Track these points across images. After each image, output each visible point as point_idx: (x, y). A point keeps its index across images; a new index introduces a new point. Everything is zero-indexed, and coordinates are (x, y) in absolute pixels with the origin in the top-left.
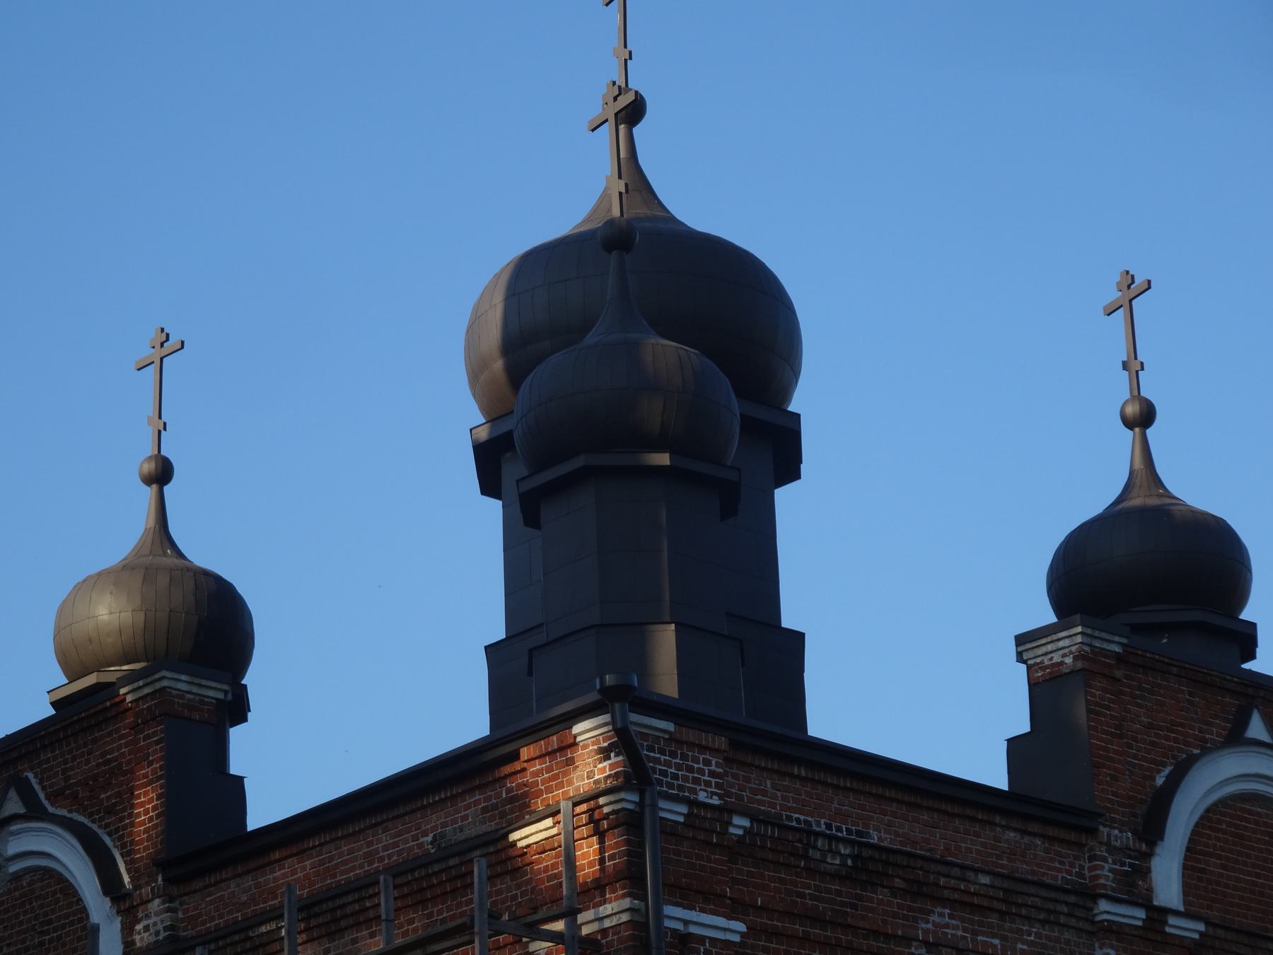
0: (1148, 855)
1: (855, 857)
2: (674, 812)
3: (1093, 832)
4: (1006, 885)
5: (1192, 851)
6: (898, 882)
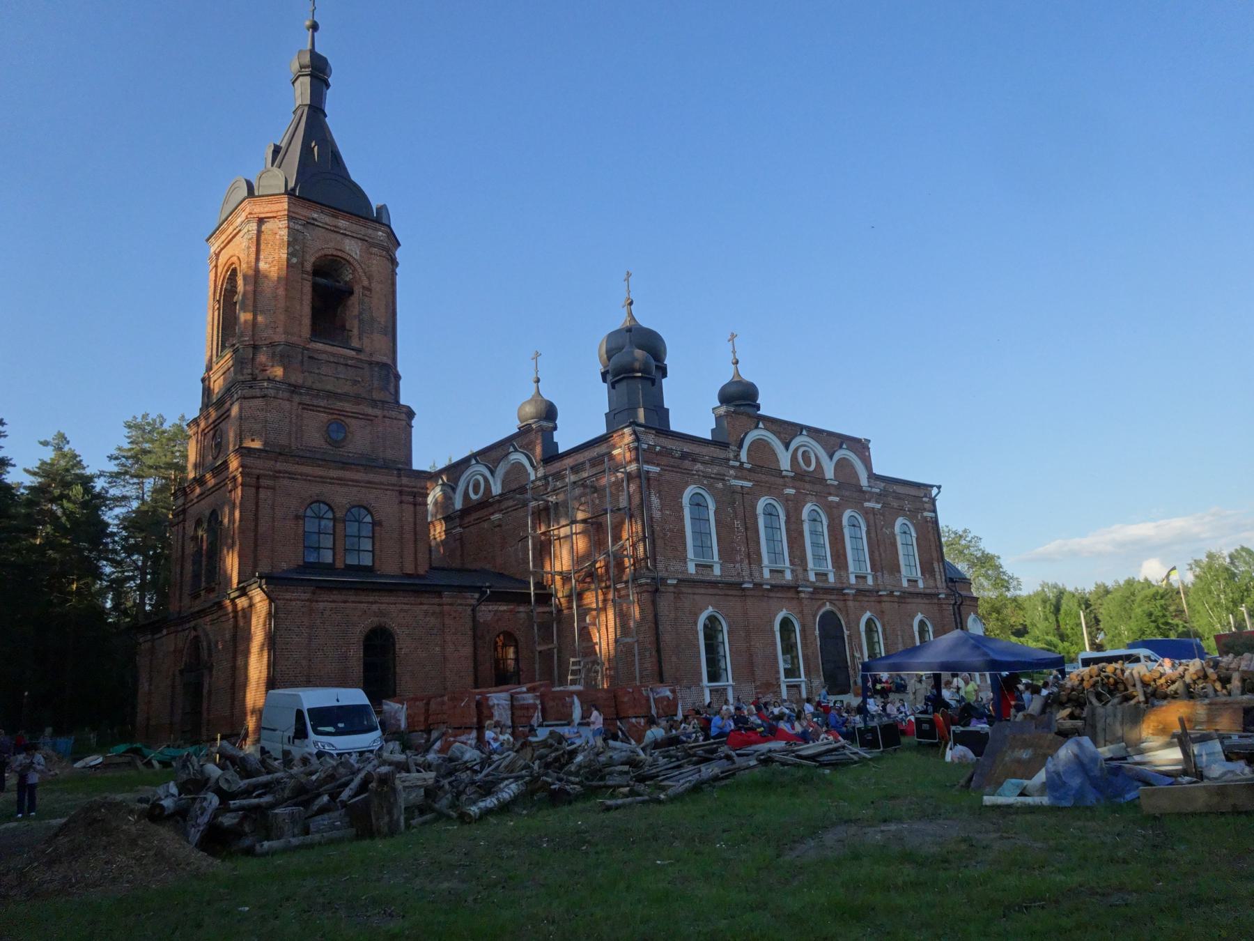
2: (645, 446)
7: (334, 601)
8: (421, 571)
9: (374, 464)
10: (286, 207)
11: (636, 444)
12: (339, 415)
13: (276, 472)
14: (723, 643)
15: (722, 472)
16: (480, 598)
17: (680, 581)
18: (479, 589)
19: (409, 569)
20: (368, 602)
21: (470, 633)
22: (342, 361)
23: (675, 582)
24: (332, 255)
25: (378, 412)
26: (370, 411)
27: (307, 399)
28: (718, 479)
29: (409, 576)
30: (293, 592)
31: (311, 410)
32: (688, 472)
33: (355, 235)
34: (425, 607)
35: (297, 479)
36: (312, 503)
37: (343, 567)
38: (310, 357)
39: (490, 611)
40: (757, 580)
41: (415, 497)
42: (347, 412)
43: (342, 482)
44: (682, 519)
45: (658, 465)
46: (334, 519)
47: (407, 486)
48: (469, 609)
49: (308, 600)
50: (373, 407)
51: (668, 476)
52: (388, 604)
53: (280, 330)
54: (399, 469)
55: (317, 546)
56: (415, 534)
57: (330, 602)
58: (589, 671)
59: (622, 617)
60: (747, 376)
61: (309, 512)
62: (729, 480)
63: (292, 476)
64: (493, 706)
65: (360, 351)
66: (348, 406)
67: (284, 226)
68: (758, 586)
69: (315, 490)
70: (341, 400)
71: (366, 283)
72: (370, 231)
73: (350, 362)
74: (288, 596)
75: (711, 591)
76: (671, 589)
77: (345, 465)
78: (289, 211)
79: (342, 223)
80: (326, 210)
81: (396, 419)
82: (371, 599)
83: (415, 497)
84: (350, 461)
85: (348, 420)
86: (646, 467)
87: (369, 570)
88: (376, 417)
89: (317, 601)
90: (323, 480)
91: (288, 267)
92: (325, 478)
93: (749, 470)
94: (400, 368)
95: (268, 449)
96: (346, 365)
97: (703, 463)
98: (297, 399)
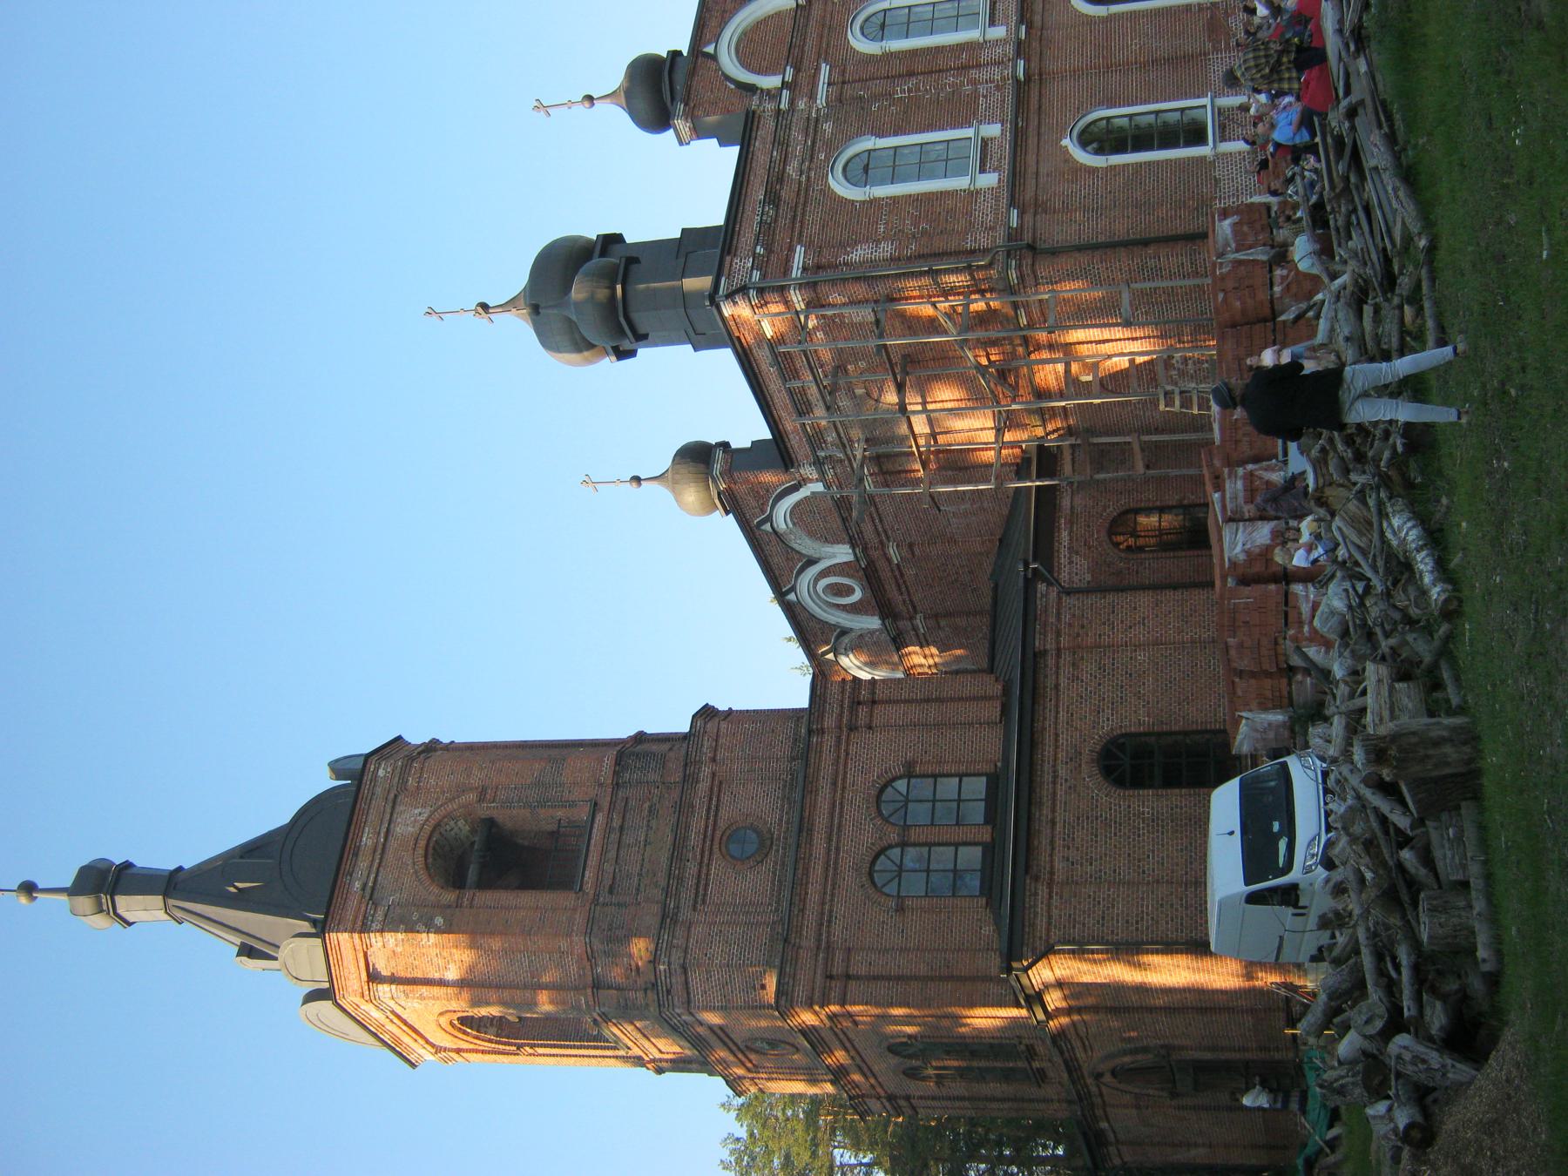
0: (762, 90)
1: (769, 205)
2: (756, 275)
3: (754, 112)
4: (776, 144)
5: (759, 72)
6: (778, 187)
7: (1052, 842)
9: (801, 779)
10: (346, 935)
11: (752, 293)
12: (712, 840)
13: (818, 948)
14: (1131, 116)
15: (802, 124)
16: (1045, 580)
17: (1012, 202)
18: (1029, 585)
19: (992, 711)
20: (1054, 783)
21: (1110, 597)
22: (614, 837)
23: (1015, 213)
24: (426, 857)
25: (706, 771)
26: (703, 786)
27: (687, 896)
28: (816, 131)
29: (1005, 710)
30: (1036, 914)
31: (706, 890)
32: (804, 191)
33: (387, 817)
34: (1063, 682)
35: (831, 911)
36: (873, 883)
37: (989, 828)
38: (611, 892)
39: (1071, 562)
40: (1010, 50)
41: (859, 703)
42: (707, 827)
44: (895, 200)
45: (791, 249)
46: (903, 845)
47: (841, 715)
51: (812, 229)
52: (1057, 747)
53: (564, 945)
54: (810, 732)
55: (951, 875)
56: (927, 701)
57: (1053, 849)
58: (1182, 374)
59: (1085, 315)
60: (616, 77)
62: (818, 110)
65: (596, 804)
66: (697, 824)
67: (379, 939)
68: (1021, 49)
70: (686, 838)
71: (472, 796)
72: (379, 790)
73: (616, 823)
74: (1041, 922)
75: (1032, 141)
76: (1028, 218)
77: (804, 828)
78: (352, 931)
79: (367, 839)
80: (346, 867)
82: (1048, 778)
84: (796, 819)
85: (722, 824)
86: (796, 272)
88: (714, 774)
89: (1052, 873)
91: (449, 933)
93: (797, 70)
94: (624, 731)
96: (622, 828)
97: (785, 161)
98: (686, 914)
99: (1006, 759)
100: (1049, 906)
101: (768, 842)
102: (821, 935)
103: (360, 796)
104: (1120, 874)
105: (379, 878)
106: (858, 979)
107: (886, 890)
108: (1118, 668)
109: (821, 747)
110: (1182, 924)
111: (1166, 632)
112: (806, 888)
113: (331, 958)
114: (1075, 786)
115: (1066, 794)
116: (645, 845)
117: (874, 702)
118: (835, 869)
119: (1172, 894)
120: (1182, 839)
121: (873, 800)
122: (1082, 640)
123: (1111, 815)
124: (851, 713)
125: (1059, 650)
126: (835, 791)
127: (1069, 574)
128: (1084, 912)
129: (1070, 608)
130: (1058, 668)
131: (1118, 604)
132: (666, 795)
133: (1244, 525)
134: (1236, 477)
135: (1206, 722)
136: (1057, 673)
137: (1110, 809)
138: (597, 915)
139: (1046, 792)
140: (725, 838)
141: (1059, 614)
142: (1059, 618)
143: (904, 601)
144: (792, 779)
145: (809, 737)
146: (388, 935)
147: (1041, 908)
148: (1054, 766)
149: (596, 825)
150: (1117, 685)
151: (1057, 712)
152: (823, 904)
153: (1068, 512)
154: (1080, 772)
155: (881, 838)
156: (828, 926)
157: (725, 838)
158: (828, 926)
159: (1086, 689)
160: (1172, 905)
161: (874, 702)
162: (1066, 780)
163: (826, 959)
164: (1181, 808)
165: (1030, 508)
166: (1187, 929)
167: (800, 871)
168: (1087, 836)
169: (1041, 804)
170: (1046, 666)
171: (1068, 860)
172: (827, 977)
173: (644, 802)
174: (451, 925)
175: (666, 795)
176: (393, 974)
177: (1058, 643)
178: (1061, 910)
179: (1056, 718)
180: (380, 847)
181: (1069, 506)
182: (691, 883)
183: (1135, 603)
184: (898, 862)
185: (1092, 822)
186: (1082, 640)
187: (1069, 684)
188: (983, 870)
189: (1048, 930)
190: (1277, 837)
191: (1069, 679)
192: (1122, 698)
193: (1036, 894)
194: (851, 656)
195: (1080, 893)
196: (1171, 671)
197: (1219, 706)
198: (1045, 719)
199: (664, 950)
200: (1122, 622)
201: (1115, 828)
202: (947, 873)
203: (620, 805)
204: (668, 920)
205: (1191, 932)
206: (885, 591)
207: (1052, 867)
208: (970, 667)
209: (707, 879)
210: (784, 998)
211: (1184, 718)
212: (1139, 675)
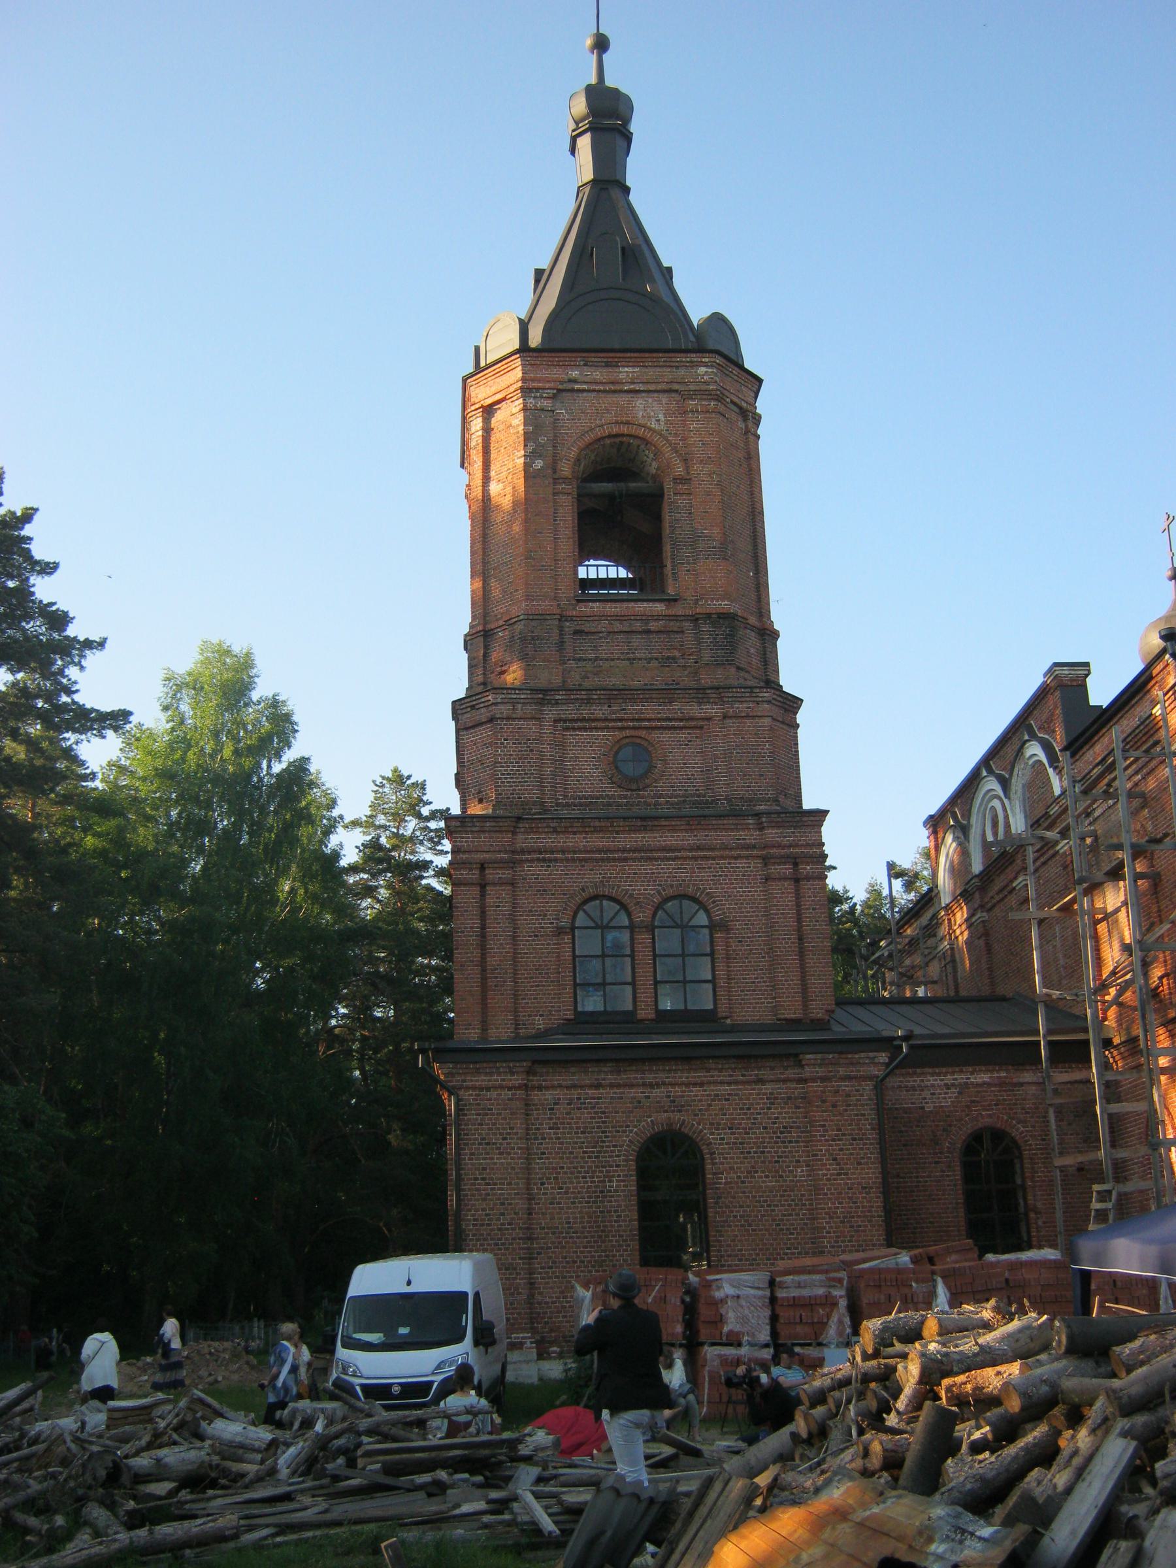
7: (574, 1086)
8: (817, 1013)
9: (707, 812)
10: (520, 375)
12: (634, 728)
13: (513, 852)
16: (892, 1060)
19: (792, 1011)
20: (644, 1085)
21: (872, 1135)
22: (638, 626)
24: (610, 436)
25: (712, 710)
26: (695, 710)
27: (570, 711)
29: (794, 1024)
30: (491, 1074)
31: (580, 729)
33: (652, 387)
34: (768, 1088)
35: (556, 860)
36: (585, 902)
37: (653, 1016)
38: (576, 632)
39: (948, 1087)
41: (796, 864)
42: (649, 720)
43: (646, 854)
46: (632, 928)
47: (779, 846)
48: (868, 1087)
49: (519, 1088)
50: (700, 703)
52: (687, 1085)
53: (519, 595)
54: (757, 815)
55: (599, 980)
56: (800, 939)
57: (568, 1088)
61: (581, 919)
63: (544, 856)
64: (723, 1301)
65: (676, 600)
66: (650, 710)
67: (518, 409)
69: (591, 876)
70: (633, 700)
71: (679, 470)
72: (682, 372)
73: (653, 626)
74: (482, 1080)
77: (647, 821)
78: (523, 379)
79: (626, 372)
80: (593, 358)
81: (748, 716)
82: (650, 1078)
83: (796, 864)
84: (660, 812)
85: (655, 734)
87: (708, 1018)
88: (709, 719)
89: (540, 1088)
90: (605, 855)
91: (526, 478)
92: (609, 851)
94: (779, 617)
95: (500, 812)
96: (648, 632)
98: (550, 713)
99: (734, 1029)
100: (501, 1087)
101: (634, 787)
102: (529, 853)
103: (673, 355)
104: (539, 1159)
105: (585, 394)
106: (481, 896)
107: (581, 914)
108: (786, 1147)
109: (743, 829)
110: (483, 1225)
111: (830, 1199)
112: (581, 833)
113: (500, 365)
114: (640, 1107)
115: (634, 1098)
116: (629, 659)
117: (797, 881)
118: (602, 860)
119: (515, 1213)
120: (580, 1223)
121: (681, 891)
122: (817, 1106)
123: (607, 1147)
124: (782, 857)
125: (805, 1081)
126: (691, 850)
127: (933, 1086)
128: (495, 1124)
129: (857, 1091)
130: (785, 1081)
131: (865, 1144)
132: (686, 672)
133: (764, 1297)
134: (830, 1287)
135: (959, 1231)
136: (778, 1081)
137: (614, 1146)
138: (550, 622)
139: (633, 1076)
140: (638, 741)
141: (850, 1078)
142: (843, 1079)
143: (992, 897)
144: (707, 802)
145: (752, 815)
146: (521, 416)
147: (496, 1079)
148: (664, 1084)
149: (651, 604)
150: (766, 1147)
151: (729, 1084)
152: (563, 852)
153: (1015, 1080)
154: (657, 1112)
155: (637, 903)
156: (538, 860)
157: (638, 741)
158: (538, 860)
159: (760, 1114)
160: (503, 1214)
161: (797, 881)
162: (648, 1097)
163: (501, 861)
164: (616, 1221)
165: (991, 1037)
166: (477, 1230)
167: (597, 823)
168: (583, 1123)
169: (619, 1073)
170: (786, 1068)
171: (555, 1104)
172: (482, 865)
173: (679, 650)
174: (534, 477)
175: (686, 672)
176: (493, 429)
177: (814, 1080)
178: (495, 1099)
179: (722, 1083)
180: (618, 387)
181: (1021, 1080)
182: (585, 713)
183: (867, 1163)
184: (612, 924)
185: (598, 1127)
186: (817, 1106)
187: (764, 1094)
188: (686, 1011)
189: (474, 1088)
190: (389, 1330)
191: (771, 1093)
192: (750, 1153)
193: (513, 1074)
194: (954, 845)
195: (516, 1119)
196: (782, 1206)
197: (740, 1260)
198: (720, 1070)
199: (510, 696)
200: (841, 1150)
201: (593, 1152)
202: (601, 975)
203: (674, 626)
204: (541, 696)
205: (473, 1235)
206: (998, 875)
207: (547, 1088)
208: (959, 975)
209: (591, 729)
210: (458, 824)
211: (724, 1221)
212: (777, 1171)
